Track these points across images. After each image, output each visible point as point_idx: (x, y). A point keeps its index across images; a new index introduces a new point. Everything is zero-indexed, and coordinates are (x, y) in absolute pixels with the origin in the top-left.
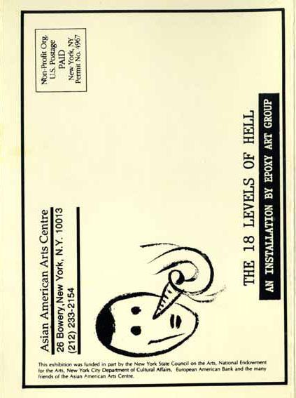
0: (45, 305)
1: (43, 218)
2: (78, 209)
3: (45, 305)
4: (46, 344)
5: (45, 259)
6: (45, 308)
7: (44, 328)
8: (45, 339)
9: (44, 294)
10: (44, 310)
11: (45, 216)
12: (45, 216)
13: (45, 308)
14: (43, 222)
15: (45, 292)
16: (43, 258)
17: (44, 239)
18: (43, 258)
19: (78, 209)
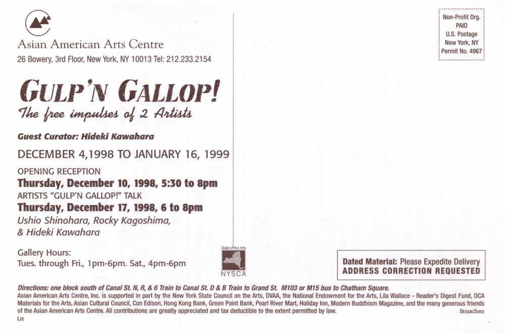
0: (66, 45)
1: (156, 44)
2: (134, 108)
3: (66, 45)
4: (26, 46)
5: (113, 46)
6: (63, 45)
7: (41, 44)
8: (31, 45)
9: (76, 44)
10: (61, 44)
11: (157, 45)
12: (157, 45)
13: (63, 45)
14: (152, 43)
15: (79, 46)
16: (115, 44)
17: (134, 44)
18: (115, 44)
19: (134, 108)
